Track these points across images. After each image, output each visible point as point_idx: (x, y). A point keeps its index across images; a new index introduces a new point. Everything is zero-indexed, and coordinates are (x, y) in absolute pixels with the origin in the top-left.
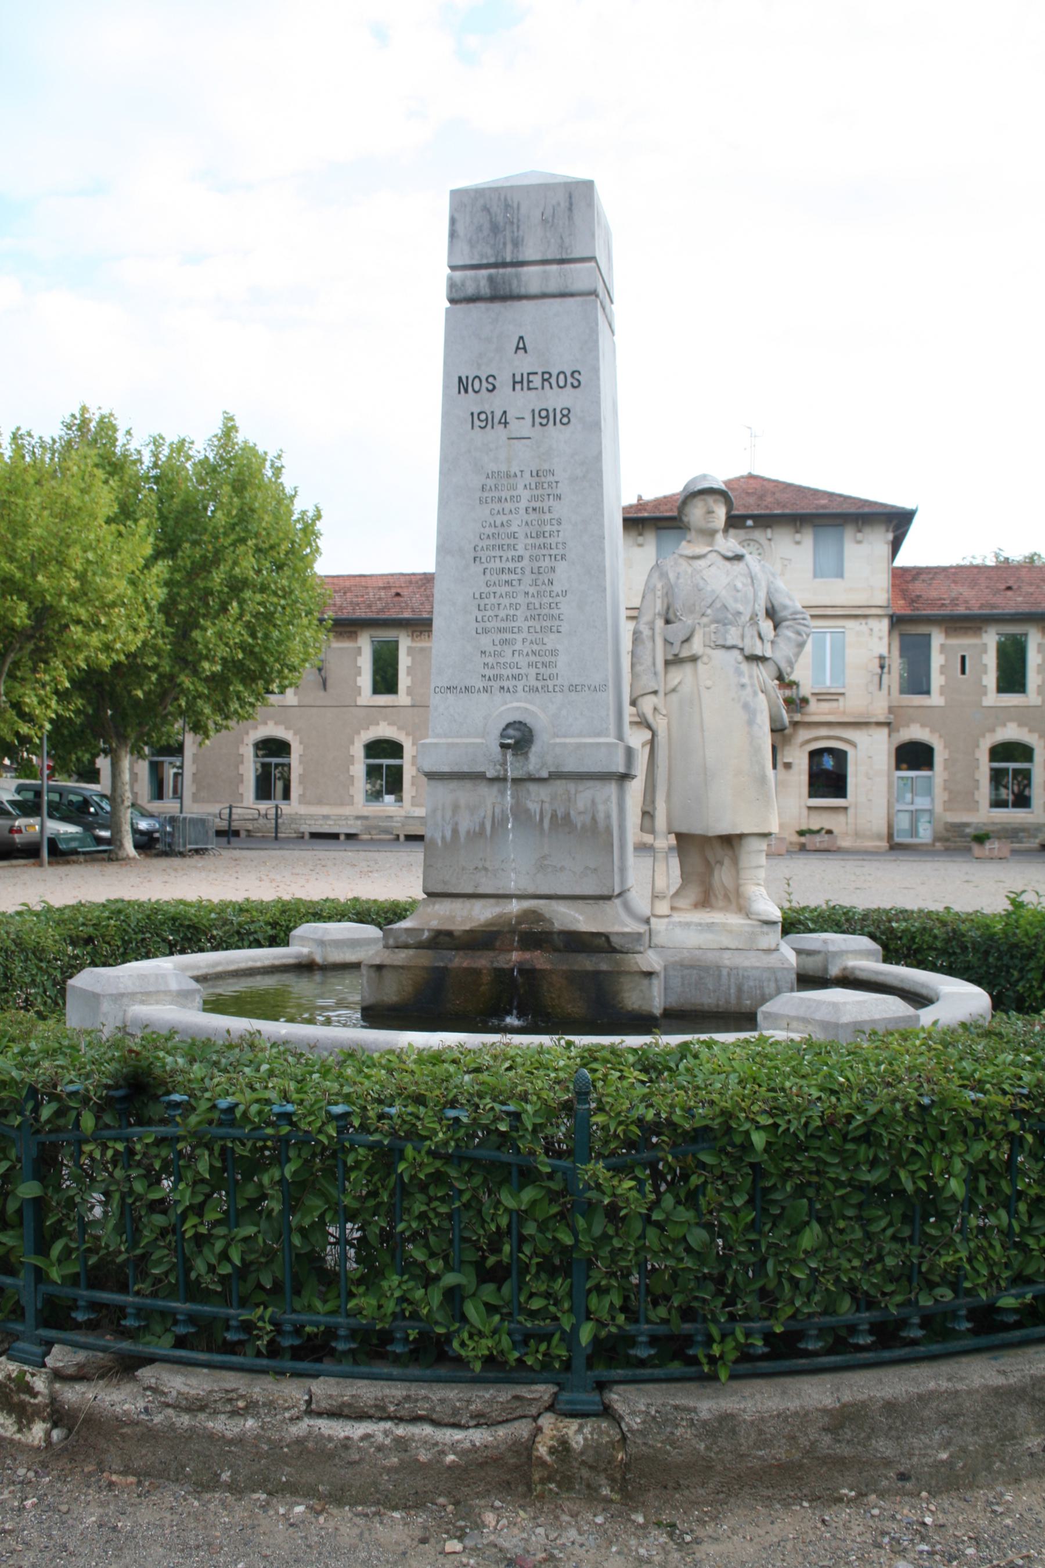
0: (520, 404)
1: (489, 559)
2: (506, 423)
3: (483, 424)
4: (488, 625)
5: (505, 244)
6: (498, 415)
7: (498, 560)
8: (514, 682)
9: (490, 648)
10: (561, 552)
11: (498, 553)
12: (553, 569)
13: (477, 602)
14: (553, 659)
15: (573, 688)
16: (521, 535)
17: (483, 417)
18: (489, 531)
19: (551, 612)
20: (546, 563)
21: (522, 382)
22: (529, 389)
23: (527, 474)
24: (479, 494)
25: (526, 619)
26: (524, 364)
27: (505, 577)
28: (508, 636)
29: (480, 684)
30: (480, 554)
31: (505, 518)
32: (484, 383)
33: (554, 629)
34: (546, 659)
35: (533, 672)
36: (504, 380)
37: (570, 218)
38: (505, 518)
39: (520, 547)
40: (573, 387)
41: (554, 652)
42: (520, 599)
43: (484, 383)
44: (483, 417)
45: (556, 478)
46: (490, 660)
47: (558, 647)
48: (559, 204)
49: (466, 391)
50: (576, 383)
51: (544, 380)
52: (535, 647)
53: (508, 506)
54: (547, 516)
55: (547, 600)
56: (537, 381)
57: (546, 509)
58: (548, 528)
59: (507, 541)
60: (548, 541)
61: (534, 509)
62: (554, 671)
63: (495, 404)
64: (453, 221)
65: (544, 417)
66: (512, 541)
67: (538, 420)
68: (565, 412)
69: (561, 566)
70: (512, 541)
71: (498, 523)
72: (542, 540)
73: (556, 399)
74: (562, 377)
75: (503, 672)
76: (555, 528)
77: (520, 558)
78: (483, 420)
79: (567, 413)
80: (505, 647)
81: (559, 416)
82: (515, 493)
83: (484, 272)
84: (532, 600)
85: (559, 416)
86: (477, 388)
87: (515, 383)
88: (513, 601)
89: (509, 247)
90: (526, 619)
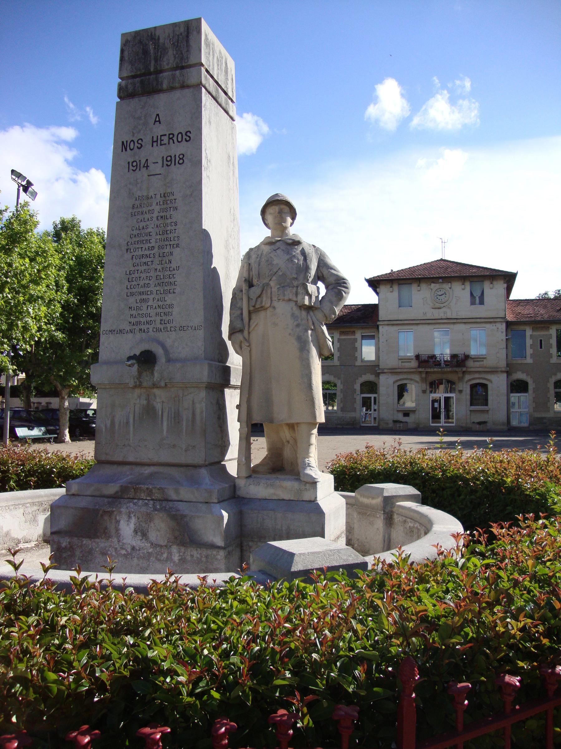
0: (156, 154)
1: (135, 249)
2: (147, 166)
3: (134, 168)
4: (134, 290)
5: (150, 61)
6: (143, 161)
7: (140, 250)
8: (148, 326)
9: (135, 305)
10: (176, 242)
11: (140, 246)
12: (171, 254)
13: (128, 276)
14: (170, 310)
15: (182, 328)
16: (153, 234)
17: (135, 164)
18: (135, 232)
19: (170, 280)
20: (167, 250)
21: (157, 141)
22: (161, 145)
23: (158, 196)
24: (131, 210)
25: (155, 286)
26: (159, 130)
27: (144, 260)
28: (144, 297)
29: (128, 328)
30: (131, 247)
31: (144, 224)
32: (136, 144)
33: (171, 291)
34: (166, 310)
35: (158, 318)
36: (147, 140)
37: (188, 41)
38: (144, 224)
39: (153, 241)
40: (186, 141)
41: (171, 306)
42: (152, 274)
43: (136, 144)
44: (135, 164)
45: (174, 197)
46: (134, 312)
47: (173, 302)
48: (181, 34)
49: (126, 150)
50: (188, 139)
51: (170, 139)
52: (160, 303)
53: (147, 216)
54: (169, 221)
55: (168, 273)
56: (165, 139)
57: (168, 216)
58: (169, 228)
59: (146, 238)
60: (169, 236)
61: (162, 217)
62: (171, 318)
63: (142, 156)
64: (122, 51)
65: (169, 161)
66: (148, 238)
67: (165, 163)
68: (181, 157)
69: (176, 251)
70: (148, 238)
71: (141, 227)
72: (165, 236)
73: (176, 149)
74: (180, 135)
75: (141, 319)
76: (173, 228)
77: (153, 247)
78: (135, 166)
79: (182, 157)
80: (143, 304)
81: (177, 159)
82: (151, 208)
83: (138, 79)
84: (159, 273)
85: (177, 159)
86: (132, 147)
87: (153, 142)
88: (148, 275)
89: (153, 63)
90: (155, 286)
